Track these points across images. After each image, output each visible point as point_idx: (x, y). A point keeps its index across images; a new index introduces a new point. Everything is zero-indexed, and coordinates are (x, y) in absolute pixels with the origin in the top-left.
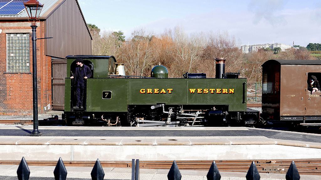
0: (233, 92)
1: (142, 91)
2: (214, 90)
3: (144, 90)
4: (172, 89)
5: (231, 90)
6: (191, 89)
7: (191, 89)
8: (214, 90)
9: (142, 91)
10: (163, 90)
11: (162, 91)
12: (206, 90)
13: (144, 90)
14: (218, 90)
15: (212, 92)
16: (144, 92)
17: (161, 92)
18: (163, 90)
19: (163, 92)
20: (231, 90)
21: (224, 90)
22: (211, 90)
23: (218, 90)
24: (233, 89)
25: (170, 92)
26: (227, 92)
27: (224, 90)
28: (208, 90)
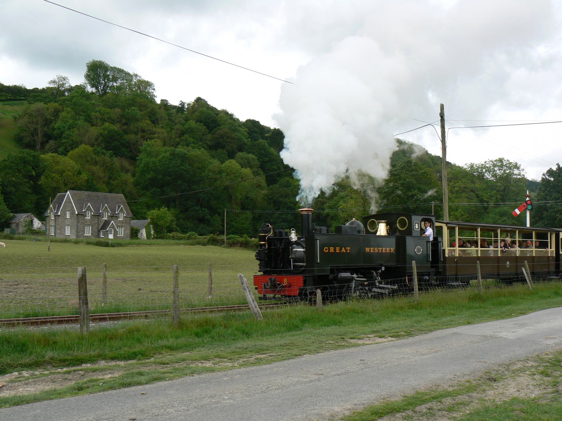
1: (326, 249)
9: (326, 249)
13: (327, 248)
15: (380, 251)
16: (327, 250)
17: (342, 251)
19: (343, 251)
25: (348, 251)
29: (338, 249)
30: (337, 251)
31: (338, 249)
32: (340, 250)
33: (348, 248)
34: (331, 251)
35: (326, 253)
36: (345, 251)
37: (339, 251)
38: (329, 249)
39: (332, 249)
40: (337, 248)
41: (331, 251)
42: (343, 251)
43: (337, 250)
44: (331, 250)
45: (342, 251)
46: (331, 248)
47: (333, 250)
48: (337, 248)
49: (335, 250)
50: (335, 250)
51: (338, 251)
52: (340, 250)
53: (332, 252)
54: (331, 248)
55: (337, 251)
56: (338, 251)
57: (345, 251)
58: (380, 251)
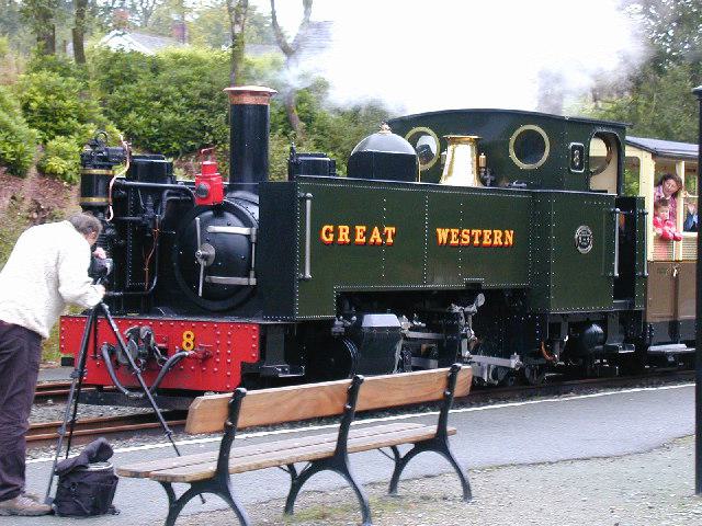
5: (507, 232)
6: (439, 230)
7: (439, 230)
9: (327, 232)
11: (373, 236)
13: (331, 228)
15: (477, 242)
16: (331, 236)
20: (507, 232)
25: (390, 240)
30: (358, 240)
32: (368, 234)
33: (390, 230)
34: (341, 239)
36: (379, 240)
41: (341, 239)
43: (359, 234)
44: (341, 234)
45: (372, 240)
48: (358, 228)
49: (352, 234)
50: (352, 234)
52: (368, 234)
53: (344, 243)
55: (358, 240)
58: (477, 242)
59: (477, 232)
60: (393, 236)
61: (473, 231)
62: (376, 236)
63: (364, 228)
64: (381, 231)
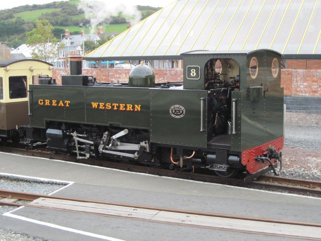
0: (139, 109)
2: (118, 105)
3: (42, 100)
4: (69, 102)
5: (136, 106)
8: (118, 105)
9: (41, 102)
10: (61, 102)
11: (60, 104)
12: (108, 105)
13: (42, 100)
14: (121, 105)
15: (115, 108)
16: (42, 103)
17: (59, 105)
18: (61, 102)
19: (61, 105)
20: (136, 106)
21: (128, 105)
22: (114, 106)
23: (121, 105)
24: (140, 106)
26: (132, 110)
27: (128, 105)
28: (110, 104)
29: (54, 102)
30: (53, 105)
31: (54, 102)
32: (58, 103)
34: (46, 104)
35: (41, 105)
36: (63, 105)
37: (56, 105)
38: (44, 102)
39: (47, 101)
40: (53, 101)
41: (46, 104)
42: (61, 105)
44: (46, 102)
45: (59, 105)
46: (46, 100)
47: (48, 103)
49: (51, 102)
50: (51, 102)
51: (54, 104)
52: (58, 103)
53: (48, 105)
54: (46, 100)
55: (53, 105)
56: (54, 104)
57: (63, 105)
58: (115, 108)
59: (116, 105)
60: (69, 104)
61: (113, 104)
62: (61, 104)
63: (56, 101)
64: (63, 102)
